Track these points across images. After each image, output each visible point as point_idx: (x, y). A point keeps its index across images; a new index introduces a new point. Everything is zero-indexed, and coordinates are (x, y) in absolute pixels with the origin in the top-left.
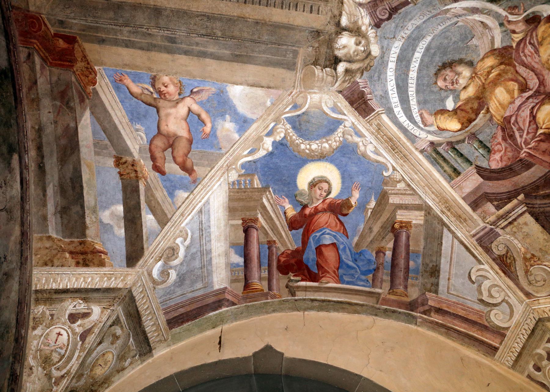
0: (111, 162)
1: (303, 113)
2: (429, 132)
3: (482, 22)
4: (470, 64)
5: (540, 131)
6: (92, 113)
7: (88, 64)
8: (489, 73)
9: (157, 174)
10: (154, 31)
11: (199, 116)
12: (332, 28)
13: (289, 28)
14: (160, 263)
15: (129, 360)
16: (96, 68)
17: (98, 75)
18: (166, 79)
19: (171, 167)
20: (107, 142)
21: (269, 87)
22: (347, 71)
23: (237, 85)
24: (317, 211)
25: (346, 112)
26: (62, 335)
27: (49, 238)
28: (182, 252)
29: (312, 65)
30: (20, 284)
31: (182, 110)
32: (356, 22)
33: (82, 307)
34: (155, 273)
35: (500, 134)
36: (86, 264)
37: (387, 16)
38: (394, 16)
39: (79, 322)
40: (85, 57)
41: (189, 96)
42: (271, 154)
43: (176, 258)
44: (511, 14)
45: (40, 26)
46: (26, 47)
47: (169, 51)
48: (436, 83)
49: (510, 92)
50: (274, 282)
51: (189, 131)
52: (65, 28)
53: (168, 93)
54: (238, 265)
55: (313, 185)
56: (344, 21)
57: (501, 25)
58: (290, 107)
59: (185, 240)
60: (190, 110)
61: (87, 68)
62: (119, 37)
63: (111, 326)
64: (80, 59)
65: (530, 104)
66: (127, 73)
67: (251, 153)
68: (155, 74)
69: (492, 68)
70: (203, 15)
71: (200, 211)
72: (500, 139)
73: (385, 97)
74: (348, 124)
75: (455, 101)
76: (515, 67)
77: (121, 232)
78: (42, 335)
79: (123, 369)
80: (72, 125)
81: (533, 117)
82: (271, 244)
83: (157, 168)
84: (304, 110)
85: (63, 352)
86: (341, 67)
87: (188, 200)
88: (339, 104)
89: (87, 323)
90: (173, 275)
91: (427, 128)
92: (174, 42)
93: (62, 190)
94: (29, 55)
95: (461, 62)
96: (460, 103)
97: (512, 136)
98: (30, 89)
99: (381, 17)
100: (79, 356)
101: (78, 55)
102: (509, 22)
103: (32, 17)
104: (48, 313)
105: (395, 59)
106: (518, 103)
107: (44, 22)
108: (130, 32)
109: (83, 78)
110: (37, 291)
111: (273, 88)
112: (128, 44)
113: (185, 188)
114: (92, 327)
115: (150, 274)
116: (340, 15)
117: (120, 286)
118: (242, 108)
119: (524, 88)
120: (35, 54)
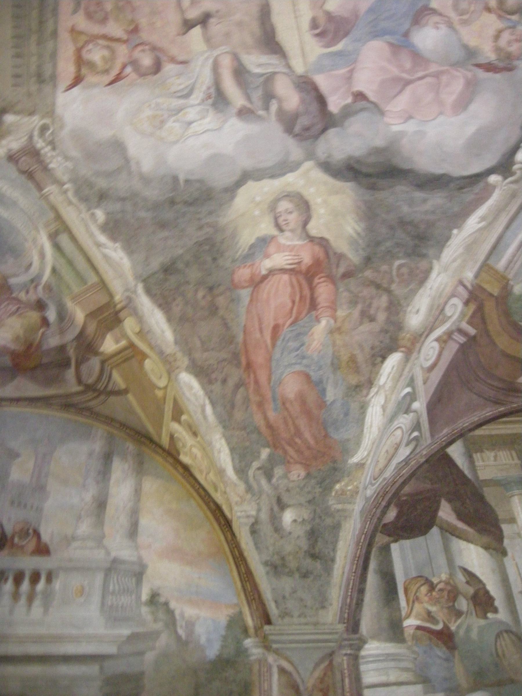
3: (30, 265)
44: (44, 288)
57: (32, 281)
102: (36, 287)
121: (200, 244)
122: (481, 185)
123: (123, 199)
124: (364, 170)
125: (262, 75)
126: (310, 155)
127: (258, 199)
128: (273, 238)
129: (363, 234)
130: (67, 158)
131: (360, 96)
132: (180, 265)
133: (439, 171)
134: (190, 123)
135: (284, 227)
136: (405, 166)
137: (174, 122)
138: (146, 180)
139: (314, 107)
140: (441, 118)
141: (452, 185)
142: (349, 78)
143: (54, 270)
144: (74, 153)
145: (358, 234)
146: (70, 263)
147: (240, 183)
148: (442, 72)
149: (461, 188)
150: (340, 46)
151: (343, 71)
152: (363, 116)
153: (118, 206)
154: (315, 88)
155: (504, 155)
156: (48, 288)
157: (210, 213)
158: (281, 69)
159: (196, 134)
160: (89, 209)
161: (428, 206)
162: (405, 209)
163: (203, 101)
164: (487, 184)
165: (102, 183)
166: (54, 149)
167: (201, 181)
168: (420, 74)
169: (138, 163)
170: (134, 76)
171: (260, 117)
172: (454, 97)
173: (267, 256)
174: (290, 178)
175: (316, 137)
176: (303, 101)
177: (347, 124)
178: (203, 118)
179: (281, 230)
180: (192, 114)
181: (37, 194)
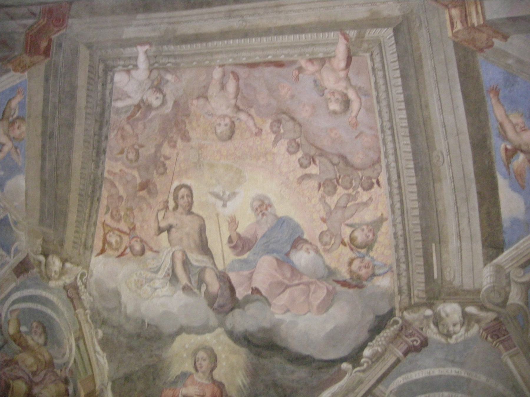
1: (11, 228)
2: (6, 315)
3: (66, 353)
4: (45, 344)
5: (11, 382)
7: (29, 67)
8: (41, 354)
10: (57, 123)
12: (64, 256)
13: (65, 225)
16: (26, 73)
17: (21, 75)
21: (26, 204)
22: (40, 262)
23: (26, 181)
25: (16, 258)
29: (43, 238)
32: (67, 273)
35: (8, 358)
37: (69, 295)
38: (69, 300)
41: (13, 144)
45: (57, 26)
46: (40, 13)
47: (43, 133)
48: (35, 321)
49: (31, 366)
52: (56, 49)
53: (14, 129)
56: (68, 265)
57: (64, 364)
58: (15, 219)
61: (25, 66)
62: (51, 95)
64: (32, 60)
65: (26, 377)
68: (26, 119)
69: (44, 356)
70: (70, 162)
72: (6, 358)
73: (26, 287)
74: (8, 259)
75: (25, 332)
76: (45, 369)
81: (19, 378)
84: (14, 228)
86: (42, 258)
88: (20, 254)
91: (9, 313)
92: (50, 138)
94: (33, 14)
95: (46, 338)
96: (24, 335)
97: (7, 365)
99: (69, 291)
101: (36, 58)
102: (66, 368)
105: (47, 296)
106: (26, 370)
109: (18, 61)
111: (26, 207)
112: (46, 101)
116: (72, 263)
119: (34, 374)
120: (36, 20)
121: (149, 367)
122: (336, 368)
123: (114, 327)
124: (255, 341)
125: (198, 267)
126: (222, 324)
127: (187, 346)
128: (191, 374)
129: (247, 386)
130: (90, 295)
131: (256, 291)
132: (135, 377)
133: (305, 352)
134: (156, 289)
135: (199, 369)
136: (282, 344)
137: (148, 286)
138: (128, 318)
139: (227, 293)
140: (308, 315)
141: (313, 365)
142: (250, 278)
143: (75, 361)
144: (94, 293)
145: (244, 386)
146: (82, 358)
147: (178, 333)
148: (312, 283)
149: (320, 368)
150: (245, 256)
151: (246, 273)
152: (258, 304)
153: (110, 330)
154: (230, 282)
155: (354, 349)
156: (71, 371)
157: (159, 348)
158: (210, 265)
159: (158, 297)
160: (96, 328)
161: (295, 376)
162: (279, 375)
163: (165, 276)
164: (340, 369)
165: (105, 314)
166: (86, 287)
167: (156, 327)
168: (296, 282)
169: (125, 307)
170: (130, 254)
171: (195, 293)
172: (319, 301)
173: (185, 386)
174: (208, 337)
175: (227, 313)
176: (220, 287)
177: (246, 308)
178: (163, 287)
179: (197, 370)
180: (157, 283)
181: (74, 311)
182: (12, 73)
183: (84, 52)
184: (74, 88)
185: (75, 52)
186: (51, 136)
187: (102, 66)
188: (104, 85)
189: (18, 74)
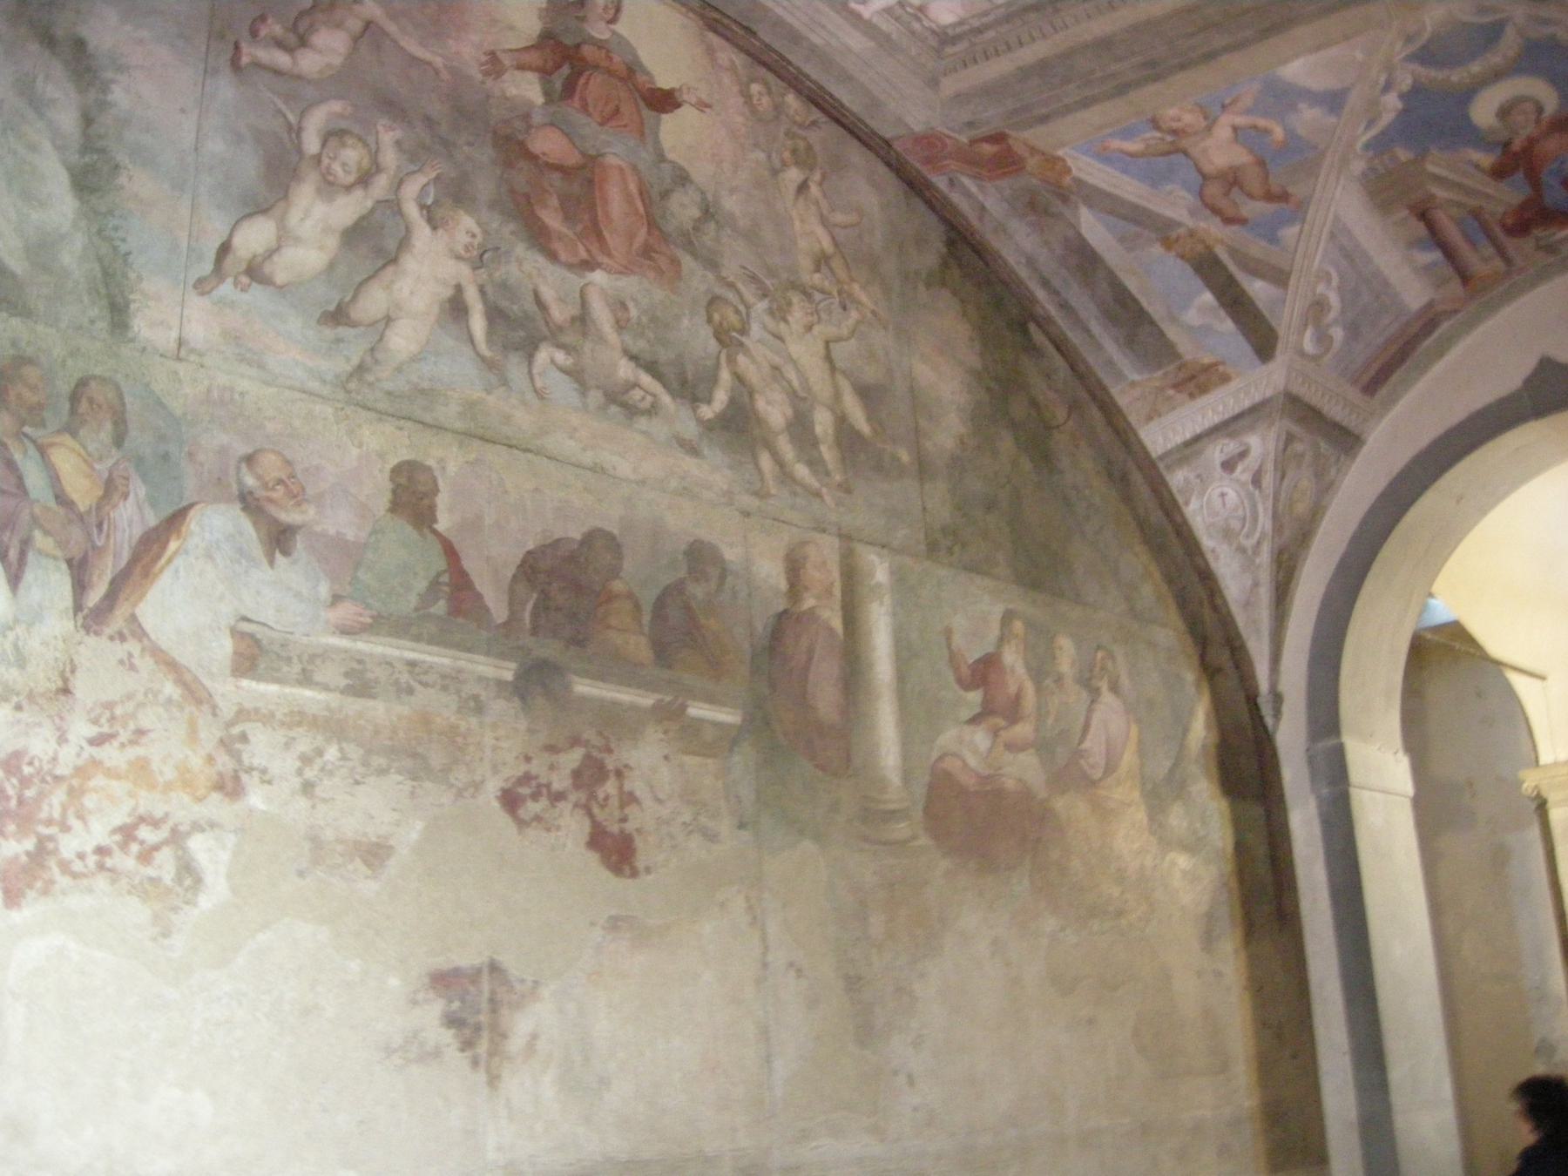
0: (1157, 250)
6: (1090, 207)
7: (1043, 154)
9: (1235, 228)
11: (1255, 127)
14: (1308, 334)
15: (1333, 471)
16: (1060, 153)
18: (1172, 112)
19: (1253, 208)
20: (1133, 229)
24: (1531, 142)
26: (1226, 494)
27: (1133, 384)
28: (1334, 299)
30: (1140, 468)
31: (1223, 132)
33: (1229, 447)
34: (1309, 345)
36: (1203, 389)
39: (1240, 468)
40: (1033, 150)
42: (1405, 112)
43: (1329, 311)
47: (1157, 78)
50: (1511, 251)
51: (1251, 151)
54: (1434, 264)
55: (1504, 112)
59: (1329, 281)
60: (1235, 129)
63: (1285, 450)
66: (1111, 135)
67: (1371, 123)
71: (1332, 236)
77: (1229, 325)
78: (1202, 506)
79: (1332, 484)
80: (1070, 233)
82: (1476, 214)
83: (1229, 221)
85: (1240, 512)
87: (1303, 236)
89: (1252, 461)
90: (1338, 334)
93: (1110, 318)
98: (981, 219)
100: (1265, 509)
103: (925, 137)
104: (1192, 476)
107: (944, 135)
108: (1079, 87)
110: (1161, 458)
112: (1086, 103)
113: (1290, 221)
114: (1260, 467)
115: (1302, 353)
117: (1269, 393)
118: (1318, 83)
182: (1075, 172)
183: (949, 86)
184: (1024, 73)
185: (960, 98)
186: (1151, 64)
187: (949, 50)
188: (979, 31)
189: (1070, 162)
